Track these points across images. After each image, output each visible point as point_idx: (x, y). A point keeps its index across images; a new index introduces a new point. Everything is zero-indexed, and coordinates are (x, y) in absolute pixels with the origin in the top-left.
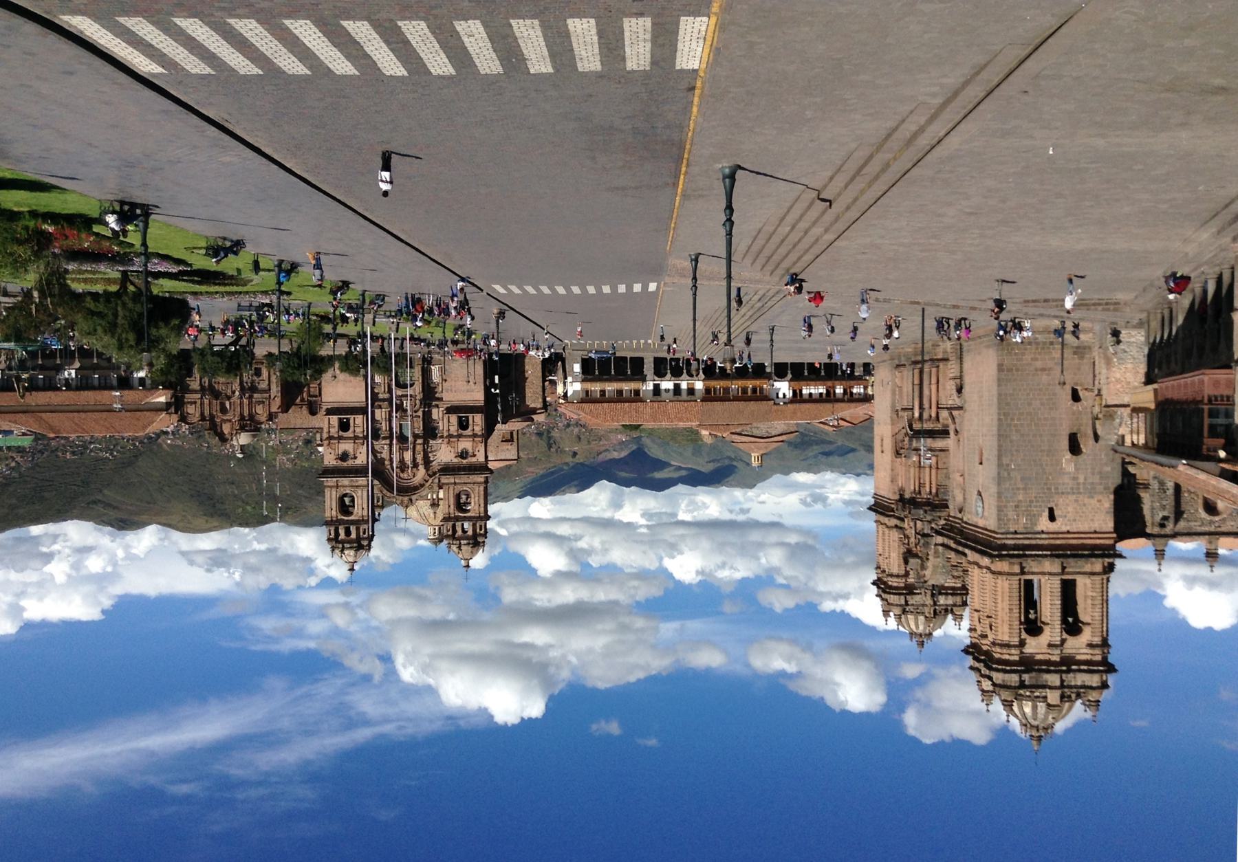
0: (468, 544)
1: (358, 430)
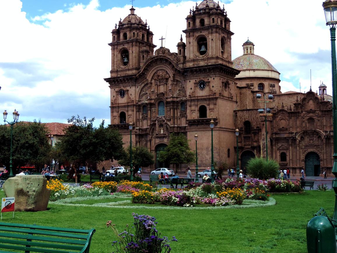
1: (193, 108)
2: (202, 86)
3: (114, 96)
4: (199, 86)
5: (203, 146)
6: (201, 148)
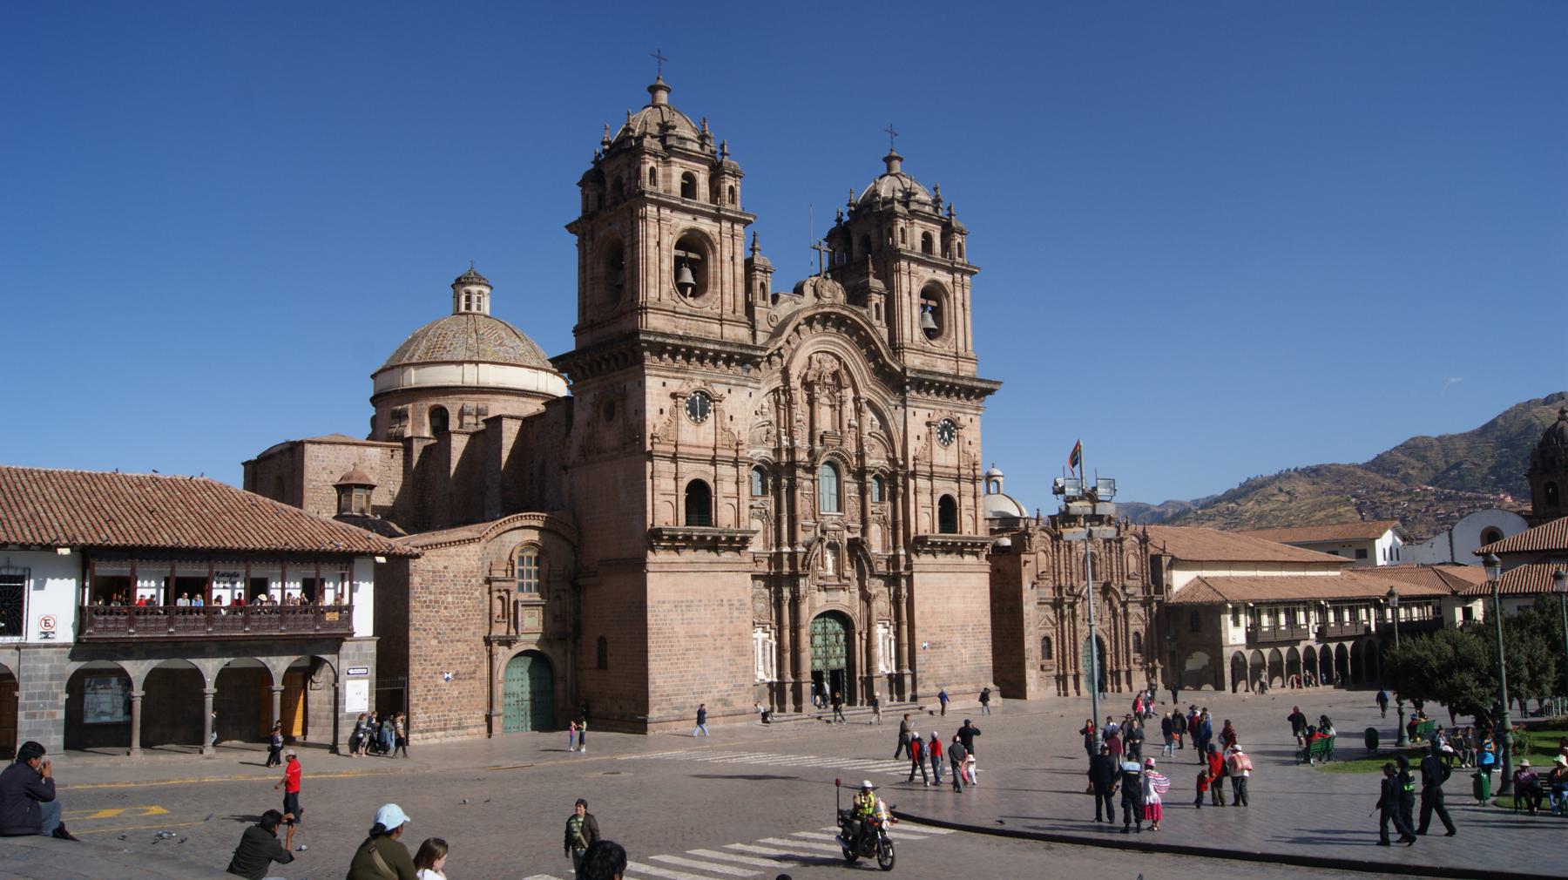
0: (682, 139)
1: (924, 499)
2: (946, 435)
3: (661, 411)
5: (953, 621)
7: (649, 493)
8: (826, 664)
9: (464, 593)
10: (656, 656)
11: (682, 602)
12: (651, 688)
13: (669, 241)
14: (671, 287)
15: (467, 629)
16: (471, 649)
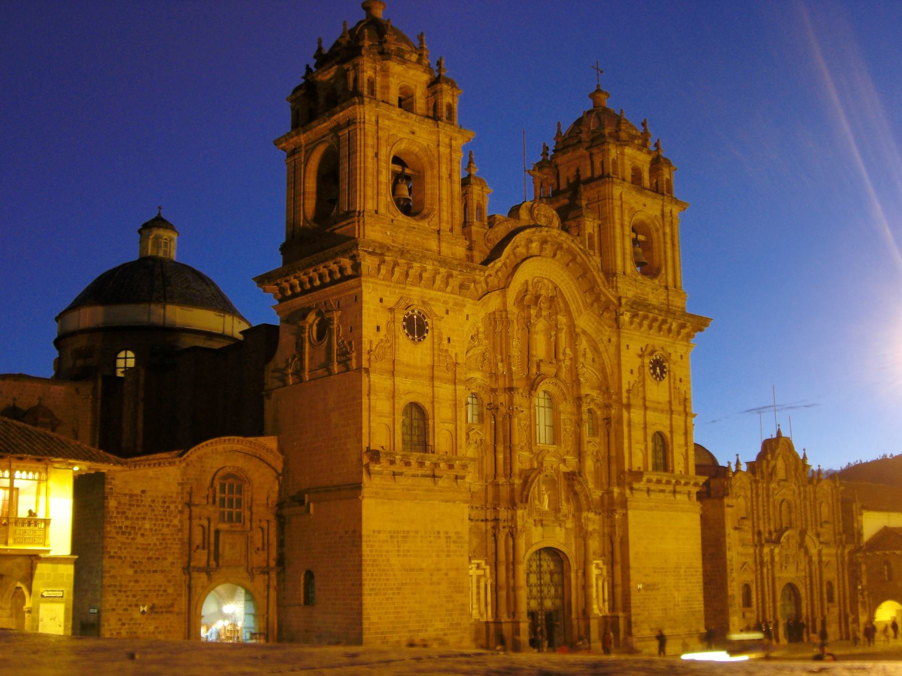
1: (638, 434)
2: (658, 371)
3: (378, 329)
4: (651, 368)
6: (662, 568)
7: (365, 414)
8: (541, 604)
9: (162, 520)
10: (371, 589)
11: (398, 532)
12: (366, 624)
13: (386, 154)
14: (389, 199)
15: (165, 559)
16: (169, 581)
